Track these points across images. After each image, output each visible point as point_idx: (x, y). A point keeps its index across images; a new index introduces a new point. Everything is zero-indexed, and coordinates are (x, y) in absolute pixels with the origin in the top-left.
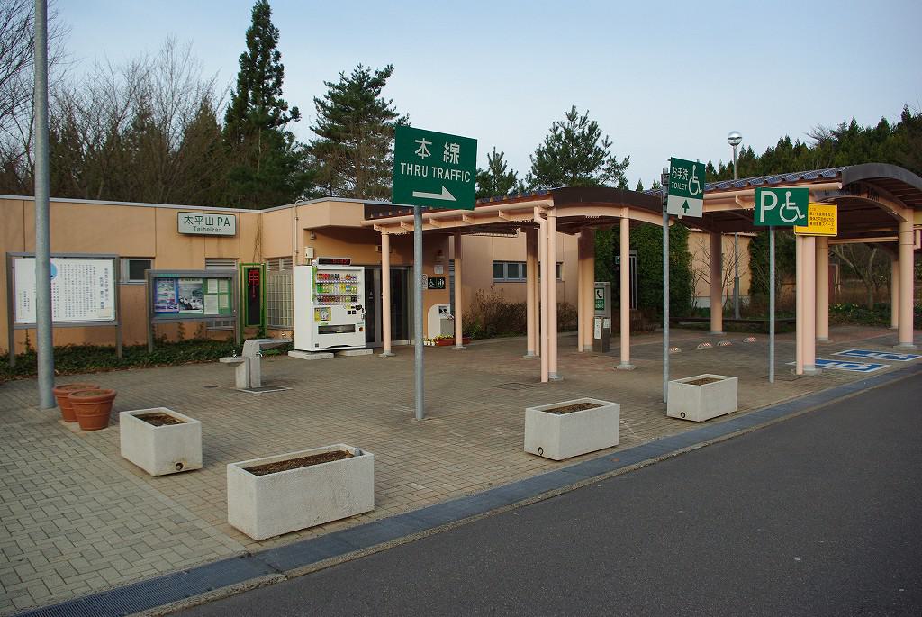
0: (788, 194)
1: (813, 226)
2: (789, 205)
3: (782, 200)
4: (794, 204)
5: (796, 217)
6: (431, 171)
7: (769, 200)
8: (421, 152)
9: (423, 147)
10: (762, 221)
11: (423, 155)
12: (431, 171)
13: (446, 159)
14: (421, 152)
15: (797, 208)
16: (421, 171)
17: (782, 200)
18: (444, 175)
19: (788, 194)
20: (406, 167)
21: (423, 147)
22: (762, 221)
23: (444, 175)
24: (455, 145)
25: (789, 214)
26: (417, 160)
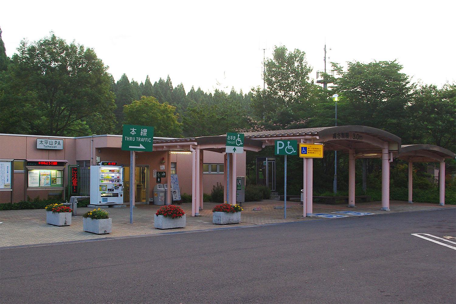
0: (289, 142)
1: (309, 154)
2: (289, 147)
3: (286, 145)
4: (291, 146)
5: (292, 152)
6: (136, 139)
7: (281, 145)
8: (132, 133)
9: (133, 131)
10: (278, 153)
11: (133, 134)
12: (136, 139)
13: (141, 134)
14: (132, 133)
15: (292, 148)
16: (132, 139)
17: (286, 145)
18: (141, 140)
19: (289, 142)
20: (127, 138)
21: (133, 131)
22: (278, 153)
23: (141, 140)
24: (145, 129)
25: (289, 150)
26: (131, 135)
